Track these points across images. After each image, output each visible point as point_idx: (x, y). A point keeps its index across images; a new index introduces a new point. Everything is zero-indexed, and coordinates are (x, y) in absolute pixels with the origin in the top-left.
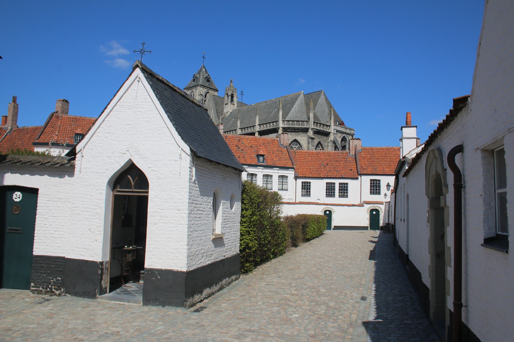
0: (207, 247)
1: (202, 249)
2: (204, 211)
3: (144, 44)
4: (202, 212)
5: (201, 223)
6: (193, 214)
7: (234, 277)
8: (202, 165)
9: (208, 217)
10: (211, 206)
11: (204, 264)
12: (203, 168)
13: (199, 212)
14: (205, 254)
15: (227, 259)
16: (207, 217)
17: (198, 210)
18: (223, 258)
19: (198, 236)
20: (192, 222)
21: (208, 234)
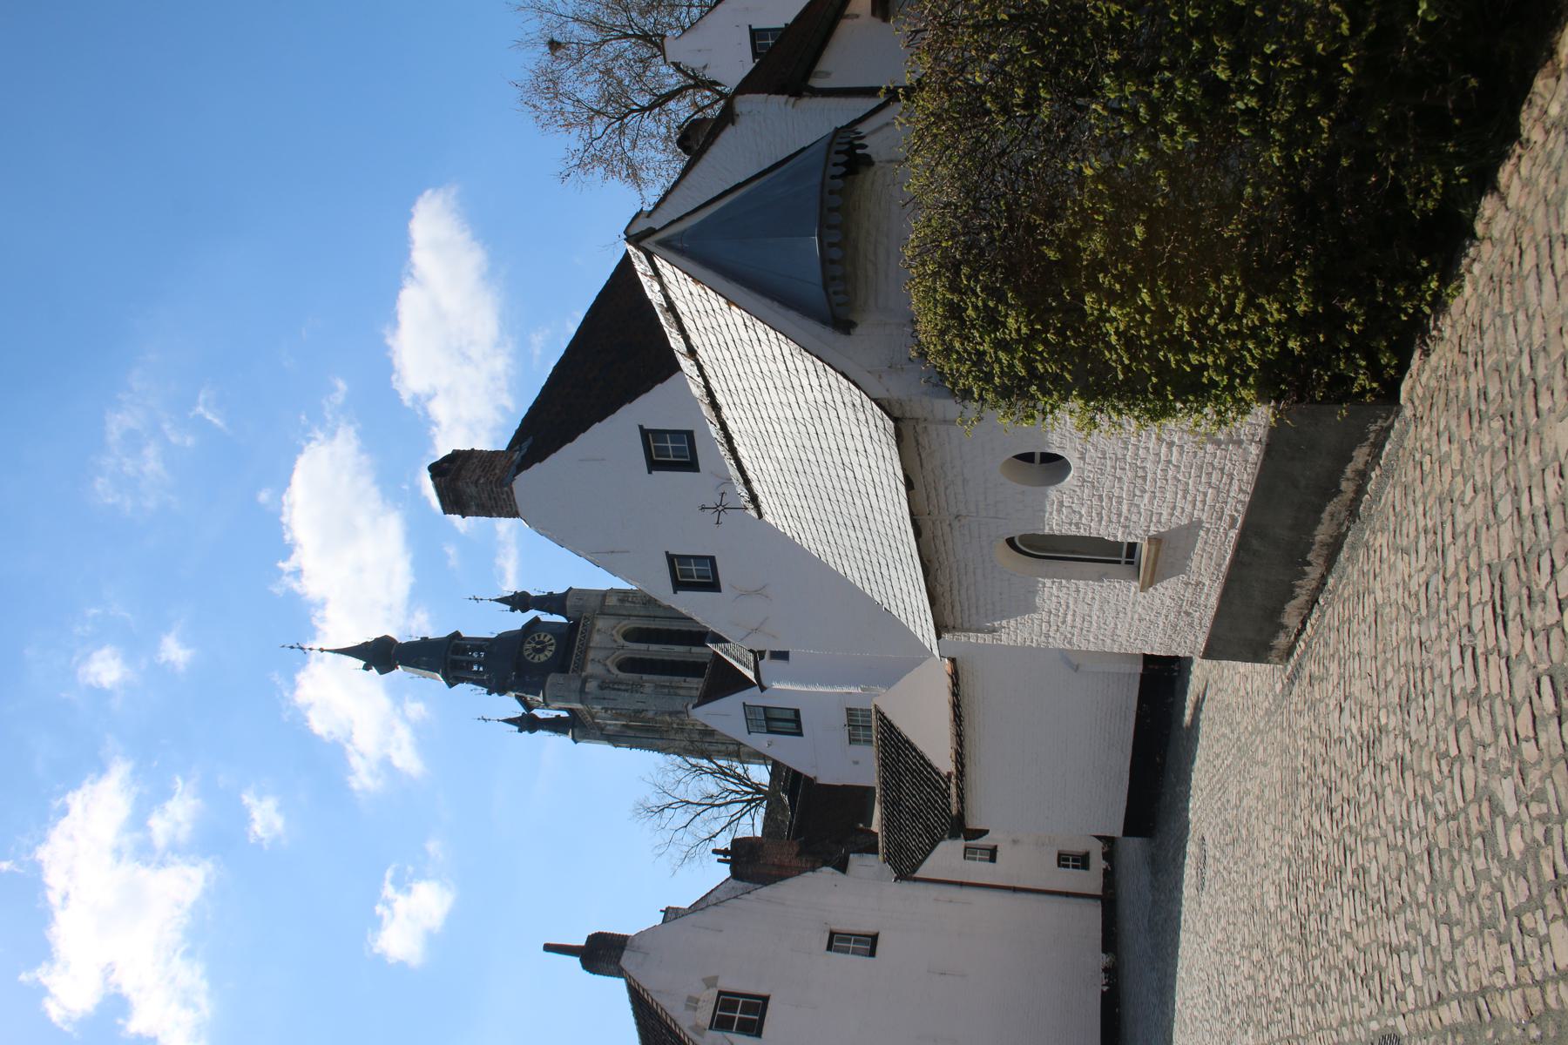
0: (1168, 601)
1: (1167, 616)
2: (1068, 607)
3: (703, 508)
4: (1070, 613)
5: (1098, 617)
6: (1073, 635)
7: (1360, 455)
8: (948, 608)
9: (1086, 593)
10: (1053, 582)
11: (1211, 613)
12: (957, 606)
13: (1069, 618)
14: (1185, 607)
15: (1252, 509)
16: (1084, 598)
17: (1064, 622)
18: (1233, 534)
19: (1127, 626)
20: (1092, 639)
21: (1132, 594)
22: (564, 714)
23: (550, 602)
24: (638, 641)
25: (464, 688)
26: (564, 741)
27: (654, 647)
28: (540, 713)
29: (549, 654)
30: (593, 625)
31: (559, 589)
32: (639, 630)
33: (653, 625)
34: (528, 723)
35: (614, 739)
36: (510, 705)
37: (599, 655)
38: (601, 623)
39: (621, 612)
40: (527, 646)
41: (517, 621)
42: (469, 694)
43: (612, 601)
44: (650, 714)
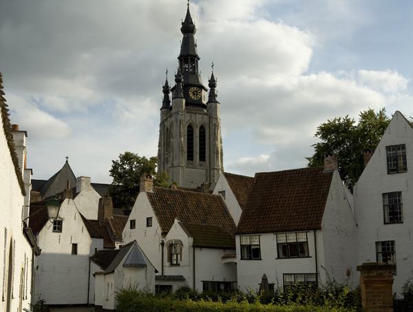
22: (171, 104)
23: (212, 96)
24: (200, 132)
26: (161, 105)
27: (198, 139)
28: (170, 95)
29: (191, 95)
30: (205, 114)
31: (217, 99)
32: (204, 133)
33: (207, 137)
34: (166, 90)
35: (162, 124)
36: (172, 84)
37: (193, 118)
38: (205, 117)
39: (211, 125)
40: (196, 88)
41: (206, 84)
42: (173, 64)
43: (214, 122)
44: (172, 140)
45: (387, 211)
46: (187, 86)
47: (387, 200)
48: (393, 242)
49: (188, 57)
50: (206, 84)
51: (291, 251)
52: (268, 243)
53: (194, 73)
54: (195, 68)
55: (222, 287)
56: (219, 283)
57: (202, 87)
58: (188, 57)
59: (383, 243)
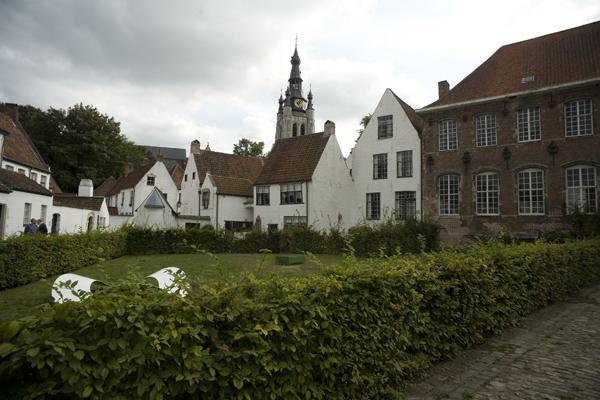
23: (310, 105)
25: (288, 84)
36: (284, 97)
45: (377, 169)
46: (293, 99)
47: (376, 160)
48: (379, 194)
49: (295, 79)
50: (306, 98)
51: (289, 199)
52: (275, 192)
53: (299, 90)
54: (300, 87)
55: (244, 225)
56: (241, 223)
57: (303, 99)
58: (295, 79)
59: (372, 194)
